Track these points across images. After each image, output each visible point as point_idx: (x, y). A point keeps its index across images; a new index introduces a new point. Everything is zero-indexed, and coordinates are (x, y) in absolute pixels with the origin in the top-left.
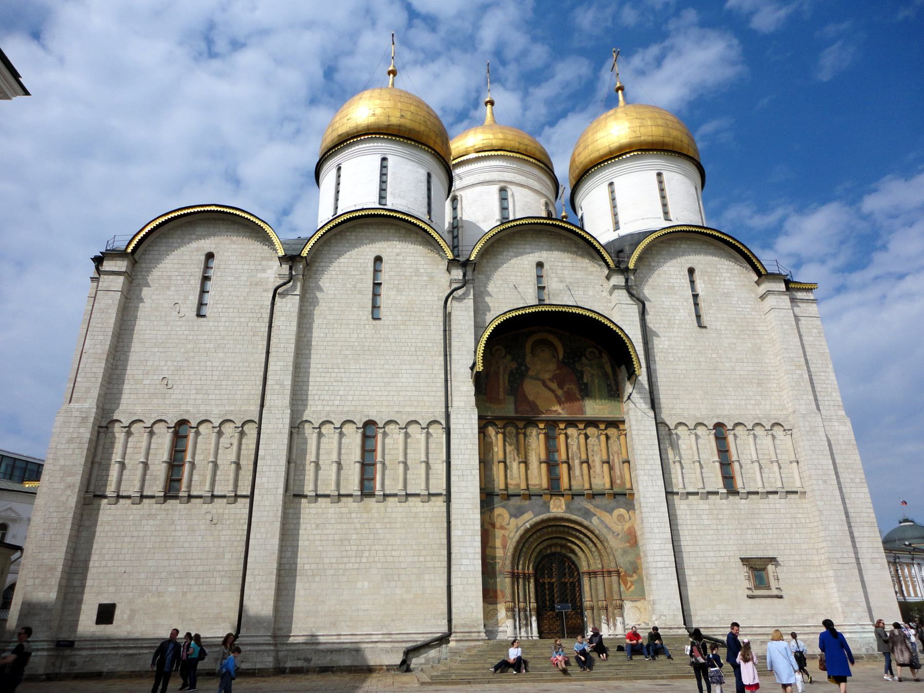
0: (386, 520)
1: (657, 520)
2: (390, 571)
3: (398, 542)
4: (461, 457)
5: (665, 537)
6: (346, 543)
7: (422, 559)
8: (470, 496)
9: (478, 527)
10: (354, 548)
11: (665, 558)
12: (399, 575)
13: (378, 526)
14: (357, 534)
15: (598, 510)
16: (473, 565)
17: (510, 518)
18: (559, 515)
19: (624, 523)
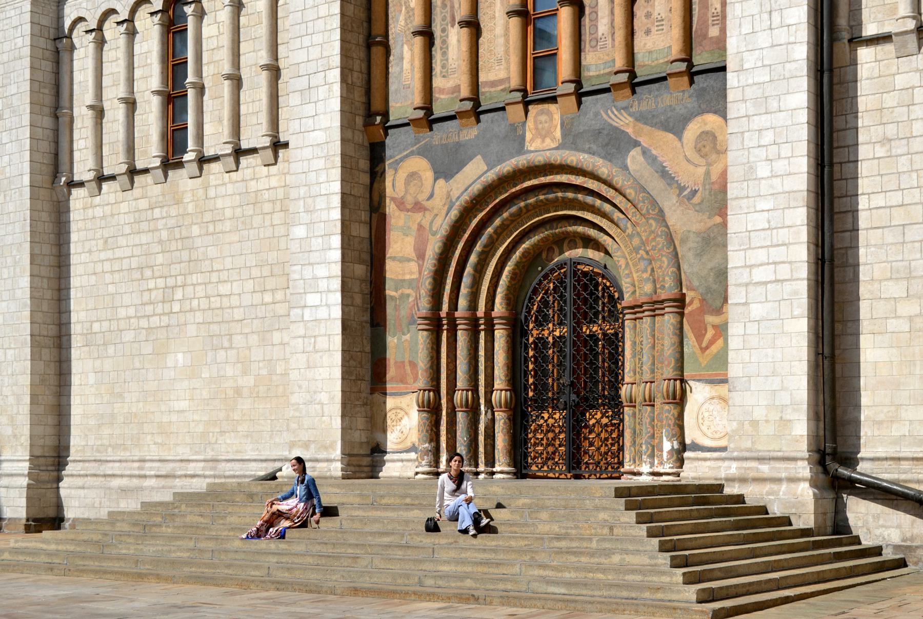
0: (208, 217)
1: (768, 137)
2: (215, 328)
3: (228, 263)
4: (306, 41)
5: (787, 189)
6: (148, 273)
7: (268, 298)
8: (319, 136)
9: (336, 214)
10: (161, 283)
11: (778, 254)
12: (231, 335)
13: (196, 230)
14: (162, 252)
15: (647, 128)
16: (326, 305)
17: (436, 179)
18: (539, 159)
19: (714, 157)
